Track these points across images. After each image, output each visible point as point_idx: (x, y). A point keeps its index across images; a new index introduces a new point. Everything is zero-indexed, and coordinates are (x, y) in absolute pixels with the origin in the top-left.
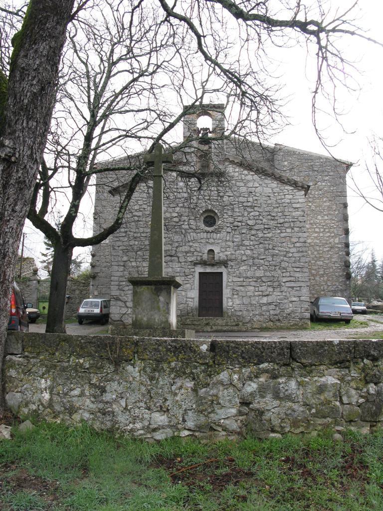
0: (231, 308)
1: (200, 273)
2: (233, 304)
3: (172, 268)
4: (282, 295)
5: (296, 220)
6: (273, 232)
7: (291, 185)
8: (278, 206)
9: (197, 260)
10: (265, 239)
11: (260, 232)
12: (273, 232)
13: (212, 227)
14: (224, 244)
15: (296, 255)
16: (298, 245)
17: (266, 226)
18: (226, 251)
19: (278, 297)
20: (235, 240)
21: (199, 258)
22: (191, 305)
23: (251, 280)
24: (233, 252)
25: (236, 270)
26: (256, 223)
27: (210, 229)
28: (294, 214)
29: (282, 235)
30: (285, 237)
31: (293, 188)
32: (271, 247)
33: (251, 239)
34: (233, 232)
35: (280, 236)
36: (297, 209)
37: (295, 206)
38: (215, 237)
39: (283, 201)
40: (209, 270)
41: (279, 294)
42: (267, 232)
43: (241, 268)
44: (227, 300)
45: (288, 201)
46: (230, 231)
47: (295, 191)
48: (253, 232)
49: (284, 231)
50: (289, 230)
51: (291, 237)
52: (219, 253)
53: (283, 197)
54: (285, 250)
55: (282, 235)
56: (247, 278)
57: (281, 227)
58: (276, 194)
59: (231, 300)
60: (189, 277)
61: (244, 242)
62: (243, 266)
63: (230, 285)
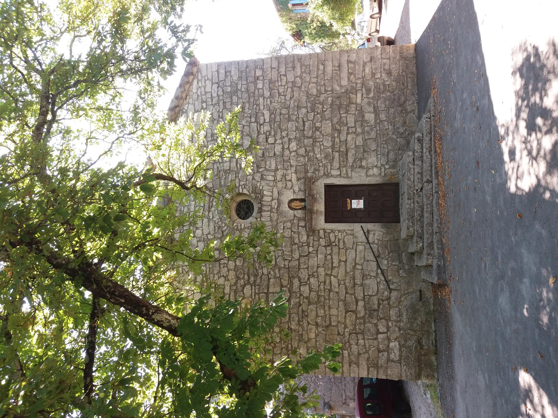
0: (383, 170)
1: (326, 221)
2: (376, 166)
3: (318, 267)
4: (362, 90)
5: (244, 74)
6: (262, 108)
7: (191, 84)
8: (221, 103)
9: (305, 226)
10: (272, 121)
11: (262, 129)
12: (262, 108)
13: (252, 204)
14: (280, 185)
15: (298, 71)
16: (283, 70)
17: (253, 120)
18: (291, 180)
19: (364, 96)
20: (273, 167)
21: (302, 224)
22: (379, 235)
23: (337, 140)
24: (293, 169)
25: (321, 164)
26: (248, 135)
27: (256, 207)
28: (235, 78)
29: (267, 94)
30: (271, 89)
31: (195, 81)
32: (284, 111)
33: (273, 142)
34: (261, 170)
35: (269, 98)
36: (228, 74)
37: (222, 77)
38: (269, 199)
39: (215, 95)
40: (321, 206)
41: (359, 95)
42: (262, 118)
43: (318, 156)
44: (370, 176)
45: (215, 86)
46: (259, 175)
47: (200, 77)
48: (262, 138)
49: (261, 91)
50: (260, 86)
51: (271, 82)
52: (294, 192)
53: (209, 95)
54: (289, 90)
55: (267, 94)
56: (333, 147)
57: (254, 97)
58: (204, 105)
59: (371, 170)
60: (333, 239)
61: (277, 153)
62: (314, 153)
63: (345, 172)
